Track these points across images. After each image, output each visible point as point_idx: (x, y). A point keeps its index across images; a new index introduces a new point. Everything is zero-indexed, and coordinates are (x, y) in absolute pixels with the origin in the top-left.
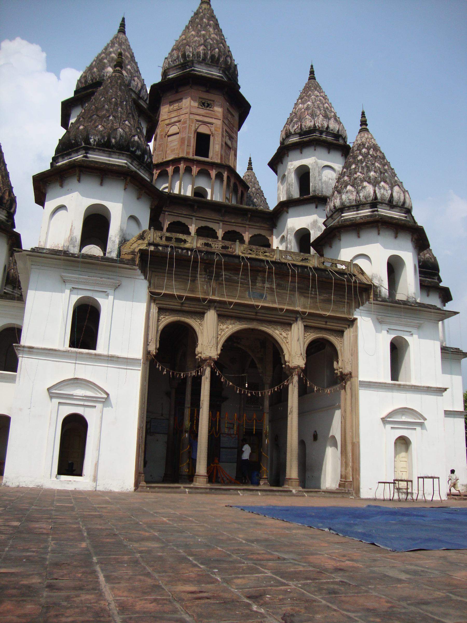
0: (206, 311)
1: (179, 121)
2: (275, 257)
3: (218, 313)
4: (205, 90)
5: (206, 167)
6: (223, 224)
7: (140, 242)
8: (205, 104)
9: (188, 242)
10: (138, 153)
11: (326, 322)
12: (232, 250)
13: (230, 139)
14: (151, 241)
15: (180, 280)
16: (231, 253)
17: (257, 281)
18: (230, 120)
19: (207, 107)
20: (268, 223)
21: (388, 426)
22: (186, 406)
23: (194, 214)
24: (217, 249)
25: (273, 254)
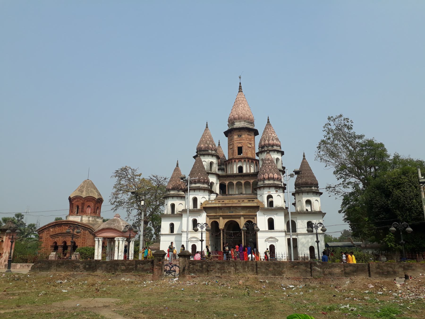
1: (232, 144)
5: (240, 160)
8: (240, 136)
10: (203, 181)
13: (250, 144)
21: (267, 242)
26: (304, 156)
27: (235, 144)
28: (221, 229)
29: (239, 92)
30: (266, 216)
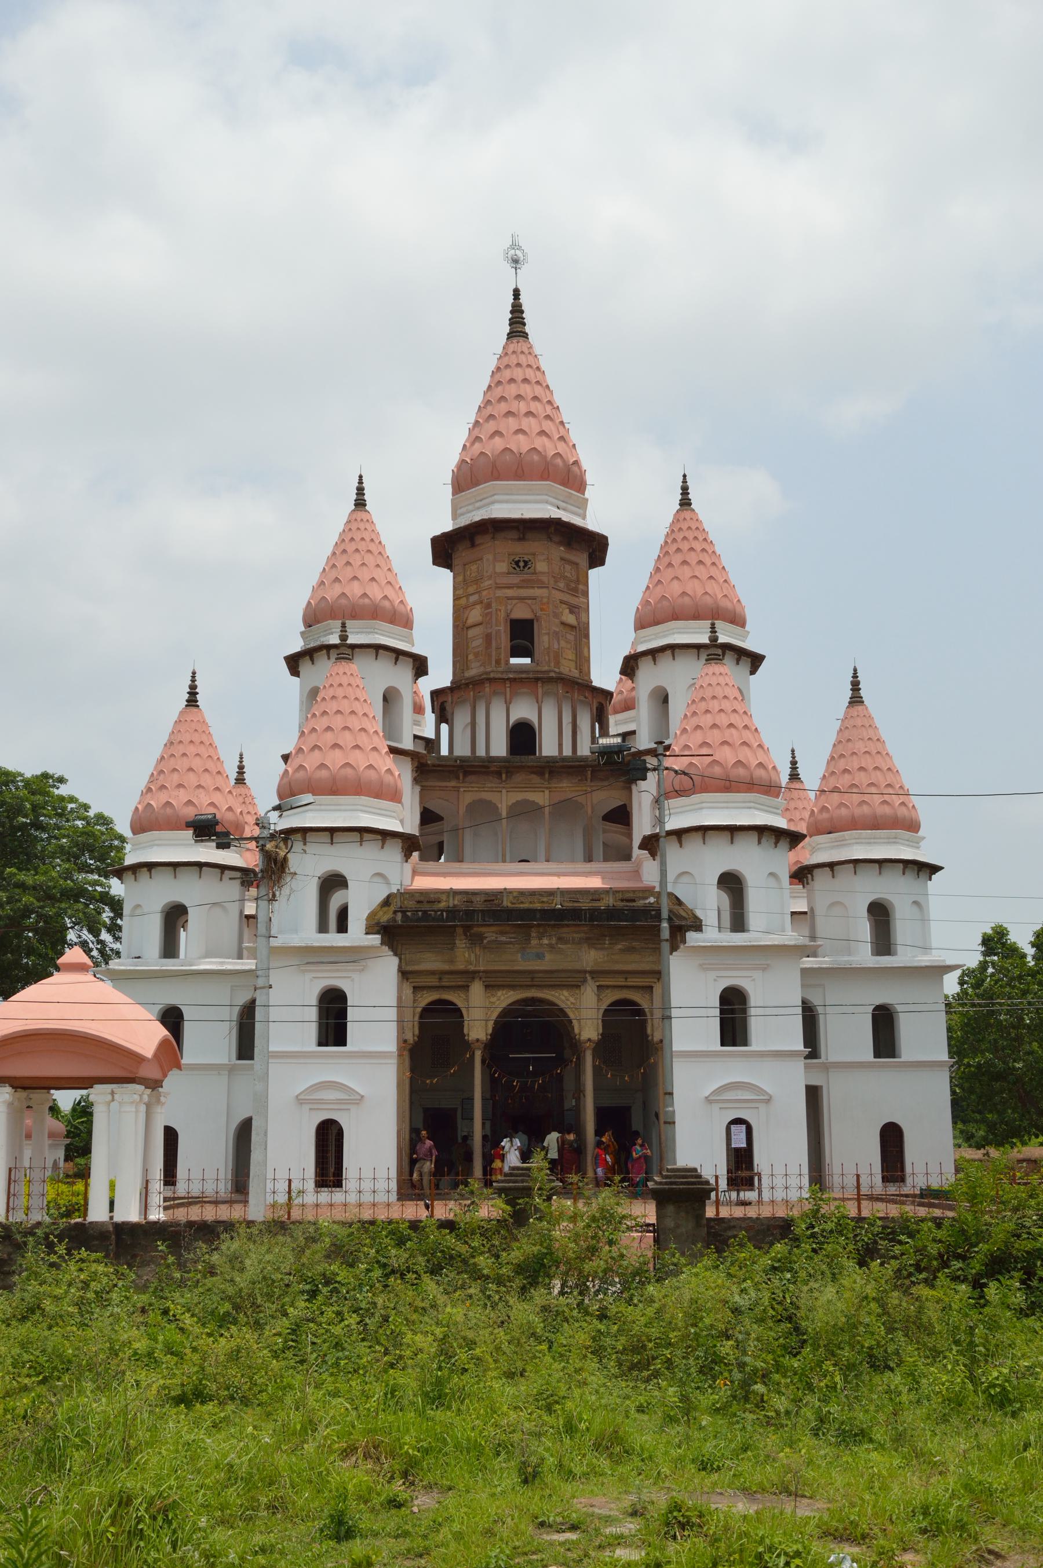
4: (516, 537)
7: (385, 909)
8: (521, 565)
11: (626, 978)
13: (571, 612)
18: (569, 575)
19: (524, 567)
21: (716, 1107)
26: (855, 686)
27: (494, 605)
28: (478, 1040)
29: (511, 335)
30: (713, 975)
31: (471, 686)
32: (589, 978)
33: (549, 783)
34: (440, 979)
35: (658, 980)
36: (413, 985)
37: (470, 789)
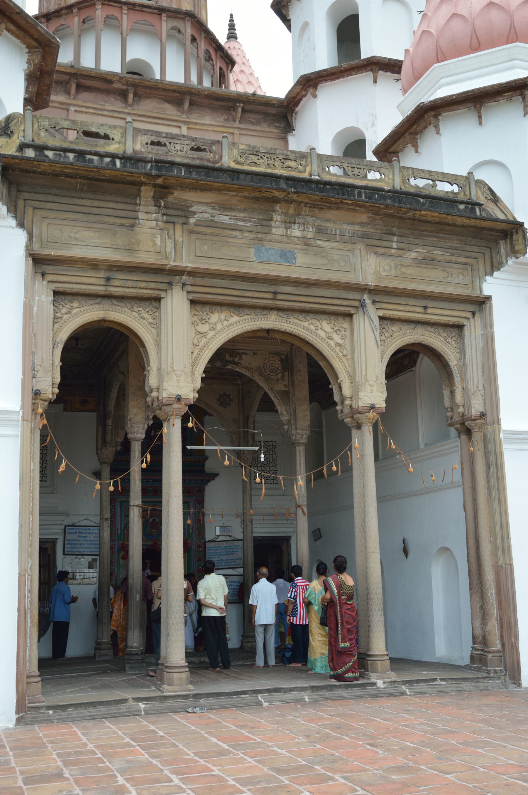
0: (163, 294)
2: (308, 169)
3: (191, 296)
6: (188, 128)
9: (113, 139)
11: (426, 308)
12: (214, 157)
14: (28, 140)
15: (101, 226)
16: (214, 162)
17: (273, 224)
20: (276, 124)
22: (132, 503)
23: (129, 110)
24: (179, 156)
25: (303, 162)
31: (75, 10)
32: (368, 302)
33: (188, 117)
34: (108, 279)
35: (474, 314)
36: (54, 286)
37: (84, 109)
